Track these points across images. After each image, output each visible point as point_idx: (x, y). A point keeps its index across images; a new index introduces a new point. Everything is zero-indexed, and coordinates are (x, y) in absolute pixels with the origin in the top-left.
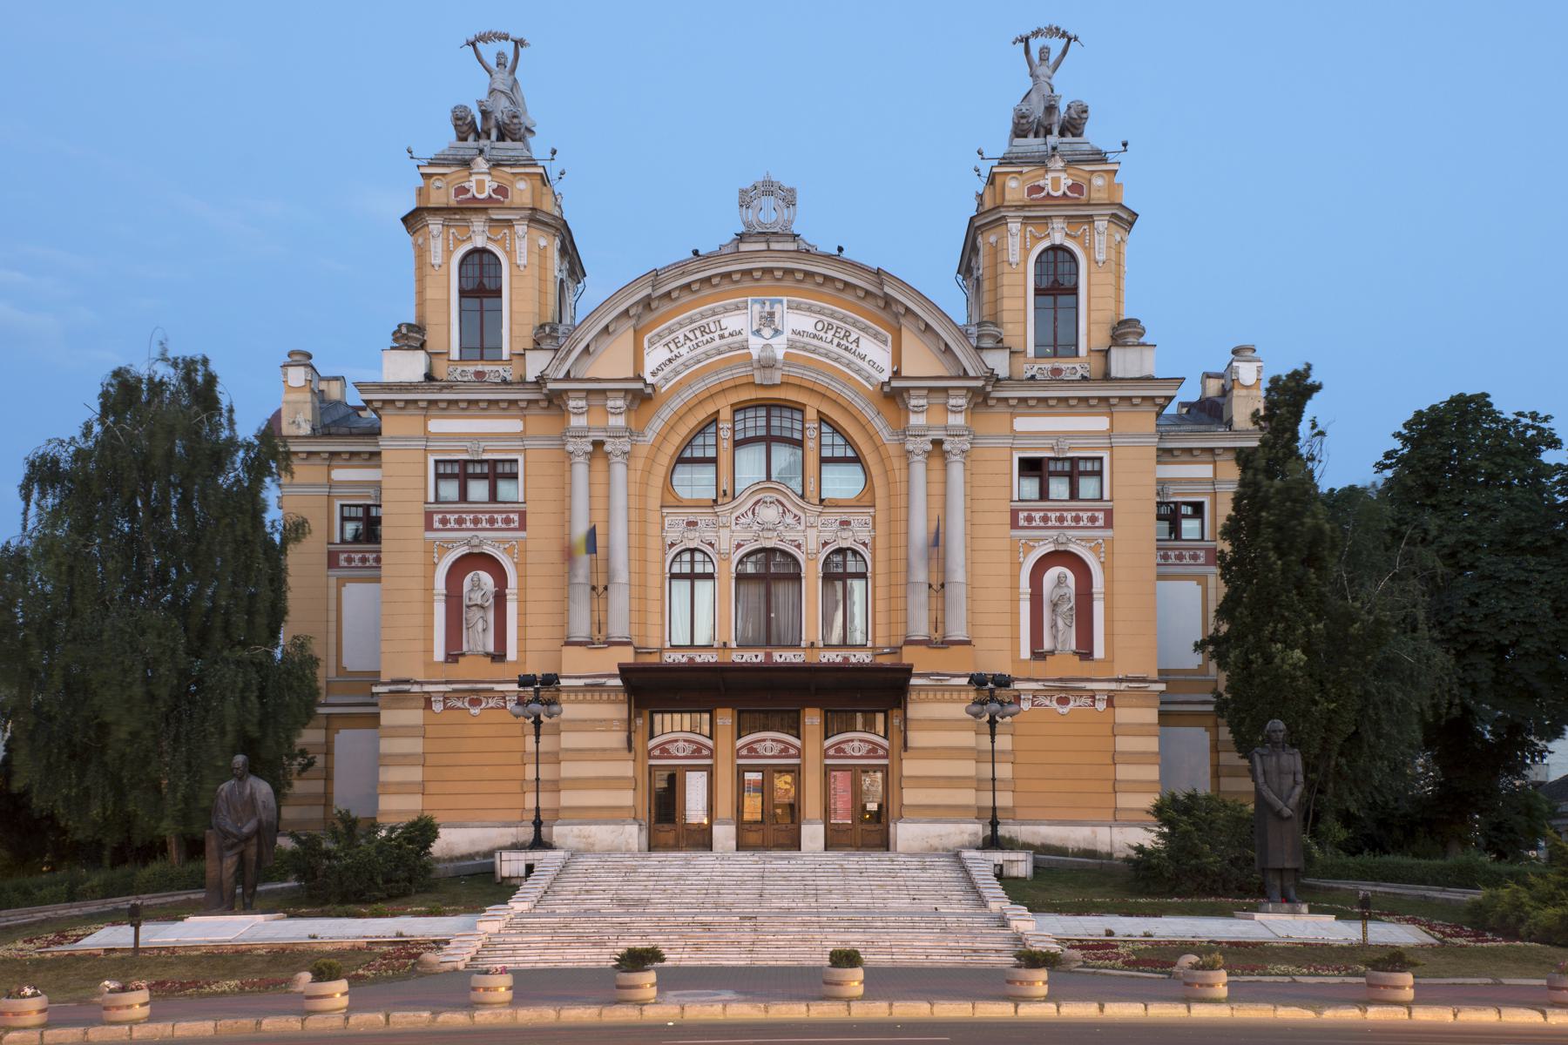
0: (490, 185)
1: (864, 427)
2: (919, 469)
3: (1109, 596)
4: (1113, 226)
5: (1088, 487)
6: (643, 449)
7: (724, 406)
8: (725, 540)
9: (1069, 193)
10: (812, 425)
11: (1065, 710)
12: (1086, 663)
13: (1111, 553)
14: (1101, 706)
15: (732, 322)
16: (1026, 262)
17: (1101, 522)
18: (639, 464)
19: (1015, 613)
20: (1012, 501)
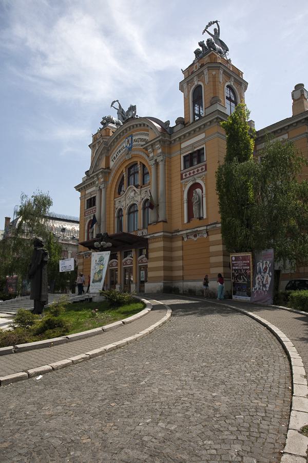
6: (109, 185)
7: (123, 168)
11: (196, 239)
14: (205, 236)
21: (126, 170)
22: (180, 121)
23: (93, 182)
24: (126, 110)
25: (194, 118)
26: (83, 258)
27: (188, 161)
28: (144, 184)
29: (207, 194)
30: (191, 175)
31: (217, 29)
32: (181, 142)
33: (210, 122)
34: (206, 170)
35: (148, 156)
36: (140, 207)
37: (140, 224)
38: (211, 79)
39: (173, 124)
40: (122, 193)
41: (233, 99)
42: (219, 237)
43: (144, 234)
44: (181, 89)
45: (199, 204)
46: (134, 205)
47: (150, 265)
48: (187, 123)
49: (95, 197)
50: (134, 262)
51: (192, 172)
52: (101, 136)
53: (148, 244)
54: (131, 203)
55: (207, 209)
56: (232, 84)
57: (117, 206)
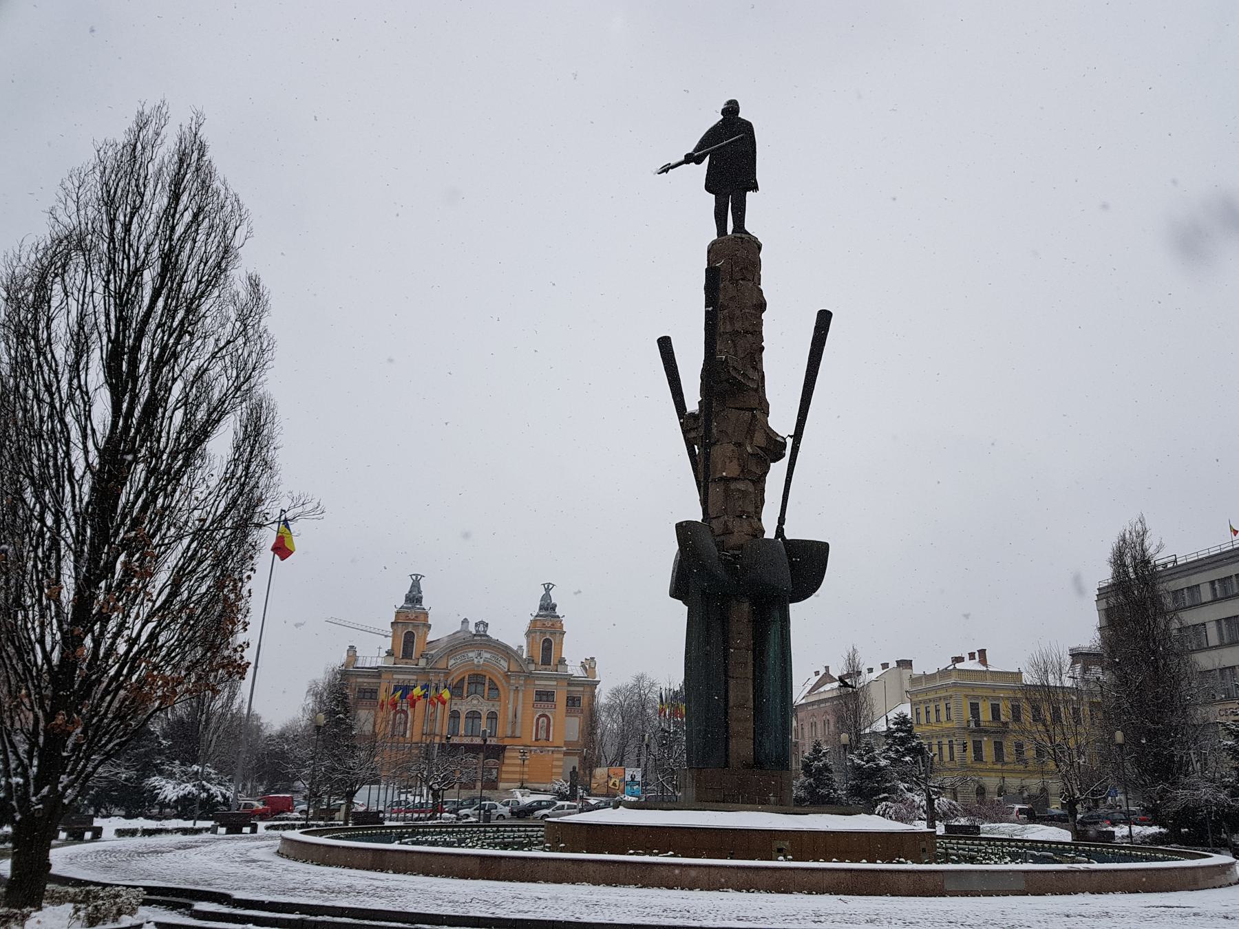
0: (414, 615)
1: (500, 681)
2: (512, 694)
3: (554, 725)
5: (550, 698)
8: (463, 708)
10: (487, 681)
15: (471, 655)
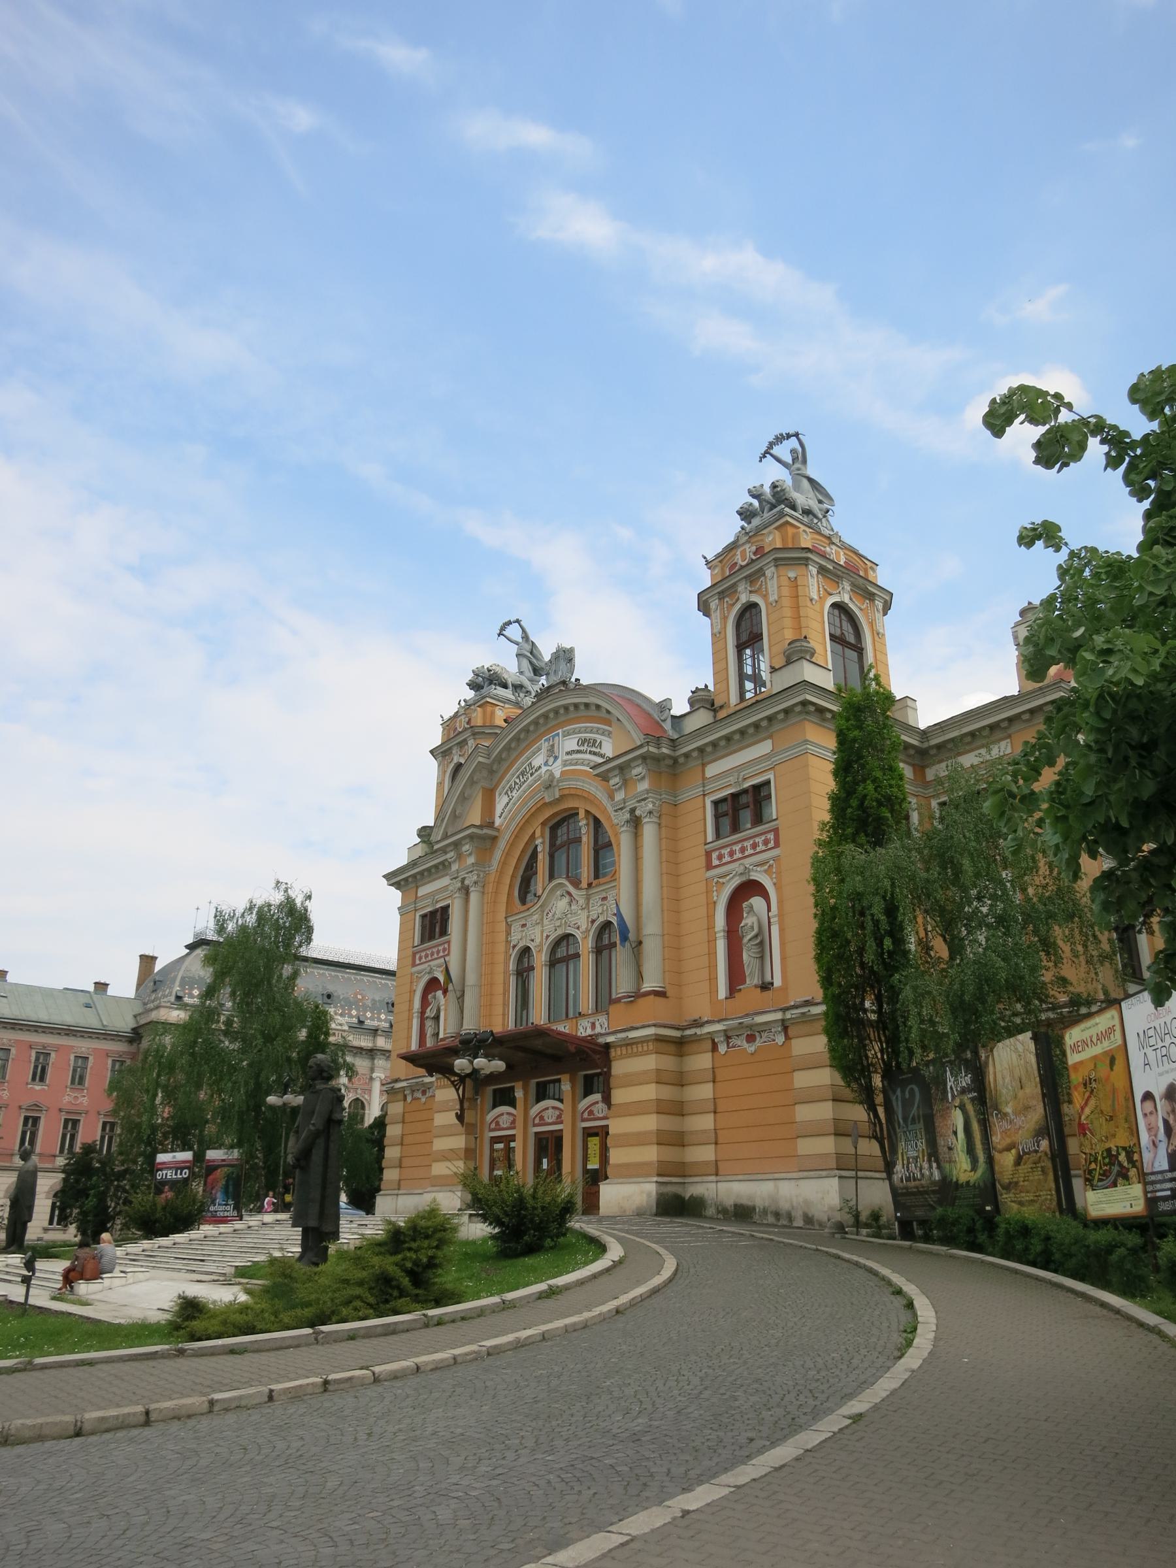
4: (780, 568)
6: (492, 878)
7: (536, 827)
9: (754, 558)
11: (751, 1048)
12: (766, 994)
13: (779, 873)
14: (780, 1039)
15: (538, 761)
16: (725, 628)
17: (772, 844)
18: (490, 888)
19: (712, 954)
20: (706, 844)
21: (542, 836)
22: (701, 700)
23: (442, 863)
24: (546, 653)
25: (742, 692)
26: (405, 1099)
27: (725, 814)
28: (597, 876)
29: (781, 915)
30: (735, 857)
31: (800, 449)
32: (705, 761)
33: (786, 711)
34: (777, 845)
35: (611, 797)
36: (586, 946)
37: (586, 998)
38: (786, 591)
39: (680, 707)
40: (530, 897)
41: (851, 639)
42: (817, 1044)
43: (598, 1030)
44: (704, 606)
45: (761, 943)
46: (567, 937)
47: (617, 1126)
48: (721, 707)
49: (448, 906)
50: (567, 1117)
51: (737, 848)
52: (468, 723)
53: (611, 1061)
54: (560, 932)
55: (783, 959)
56: (846, 599)
57: (515, 937)
